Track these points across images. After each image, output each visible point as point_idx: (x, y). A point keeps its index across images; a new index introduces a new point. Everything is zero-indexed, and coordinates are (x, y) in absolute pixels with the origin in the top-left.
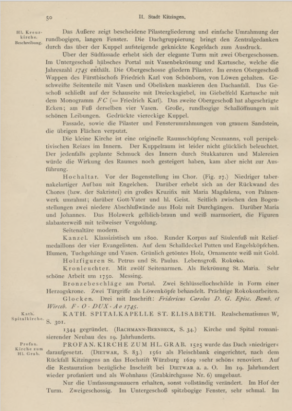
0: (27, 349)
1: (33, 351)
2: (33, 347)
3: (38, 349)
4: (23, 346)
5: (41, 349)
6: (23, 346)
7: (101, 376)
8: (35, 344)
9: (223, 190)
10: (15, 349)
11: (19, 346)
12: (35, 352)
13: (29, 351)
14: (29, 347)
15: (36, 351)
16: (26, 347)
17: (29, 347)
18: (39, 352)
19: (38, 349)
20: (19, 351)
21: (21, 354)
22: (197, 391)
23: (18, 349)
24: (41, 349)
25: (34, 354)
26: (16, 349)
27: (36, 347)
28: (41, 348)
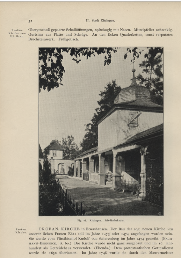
0: (16, 33)
1: (20, 35)
2: (20, 32)
3: (23, 34)
4: (13, 32)
5: (25, 33)
6: (13, 32)
7: (69, 35)
8: (21, 30)
9: (145, 31)
10: (8, 33)
11: (11, 31)
12: (21, 35)
13: (17, 35)
14: (17, 32)
15: (22, 35)
16: (15, 32)
17: (17, 32)
18: (24, 35)
19: (23, 34)
20: (11, 35)
21: (13, 36)
22: (136, 30)
23: (11, 33)
24: (25, 33)
25: (21, 37)
26: (9, 33)
27: (21, 32)
28: (25, 32)
